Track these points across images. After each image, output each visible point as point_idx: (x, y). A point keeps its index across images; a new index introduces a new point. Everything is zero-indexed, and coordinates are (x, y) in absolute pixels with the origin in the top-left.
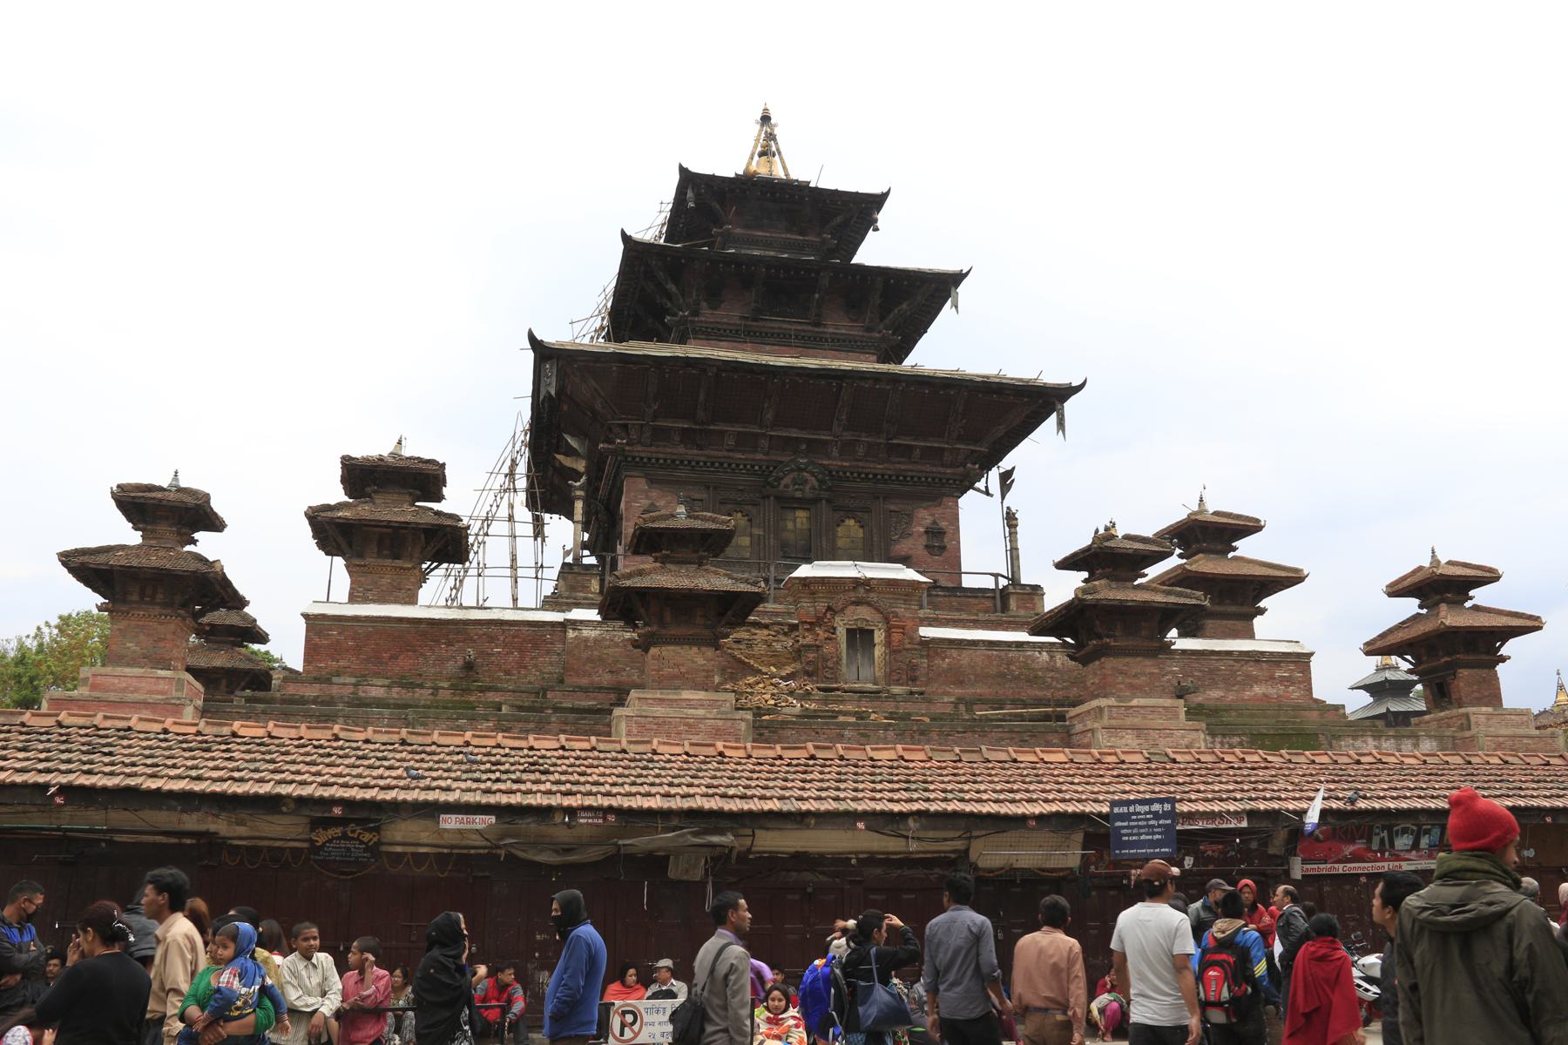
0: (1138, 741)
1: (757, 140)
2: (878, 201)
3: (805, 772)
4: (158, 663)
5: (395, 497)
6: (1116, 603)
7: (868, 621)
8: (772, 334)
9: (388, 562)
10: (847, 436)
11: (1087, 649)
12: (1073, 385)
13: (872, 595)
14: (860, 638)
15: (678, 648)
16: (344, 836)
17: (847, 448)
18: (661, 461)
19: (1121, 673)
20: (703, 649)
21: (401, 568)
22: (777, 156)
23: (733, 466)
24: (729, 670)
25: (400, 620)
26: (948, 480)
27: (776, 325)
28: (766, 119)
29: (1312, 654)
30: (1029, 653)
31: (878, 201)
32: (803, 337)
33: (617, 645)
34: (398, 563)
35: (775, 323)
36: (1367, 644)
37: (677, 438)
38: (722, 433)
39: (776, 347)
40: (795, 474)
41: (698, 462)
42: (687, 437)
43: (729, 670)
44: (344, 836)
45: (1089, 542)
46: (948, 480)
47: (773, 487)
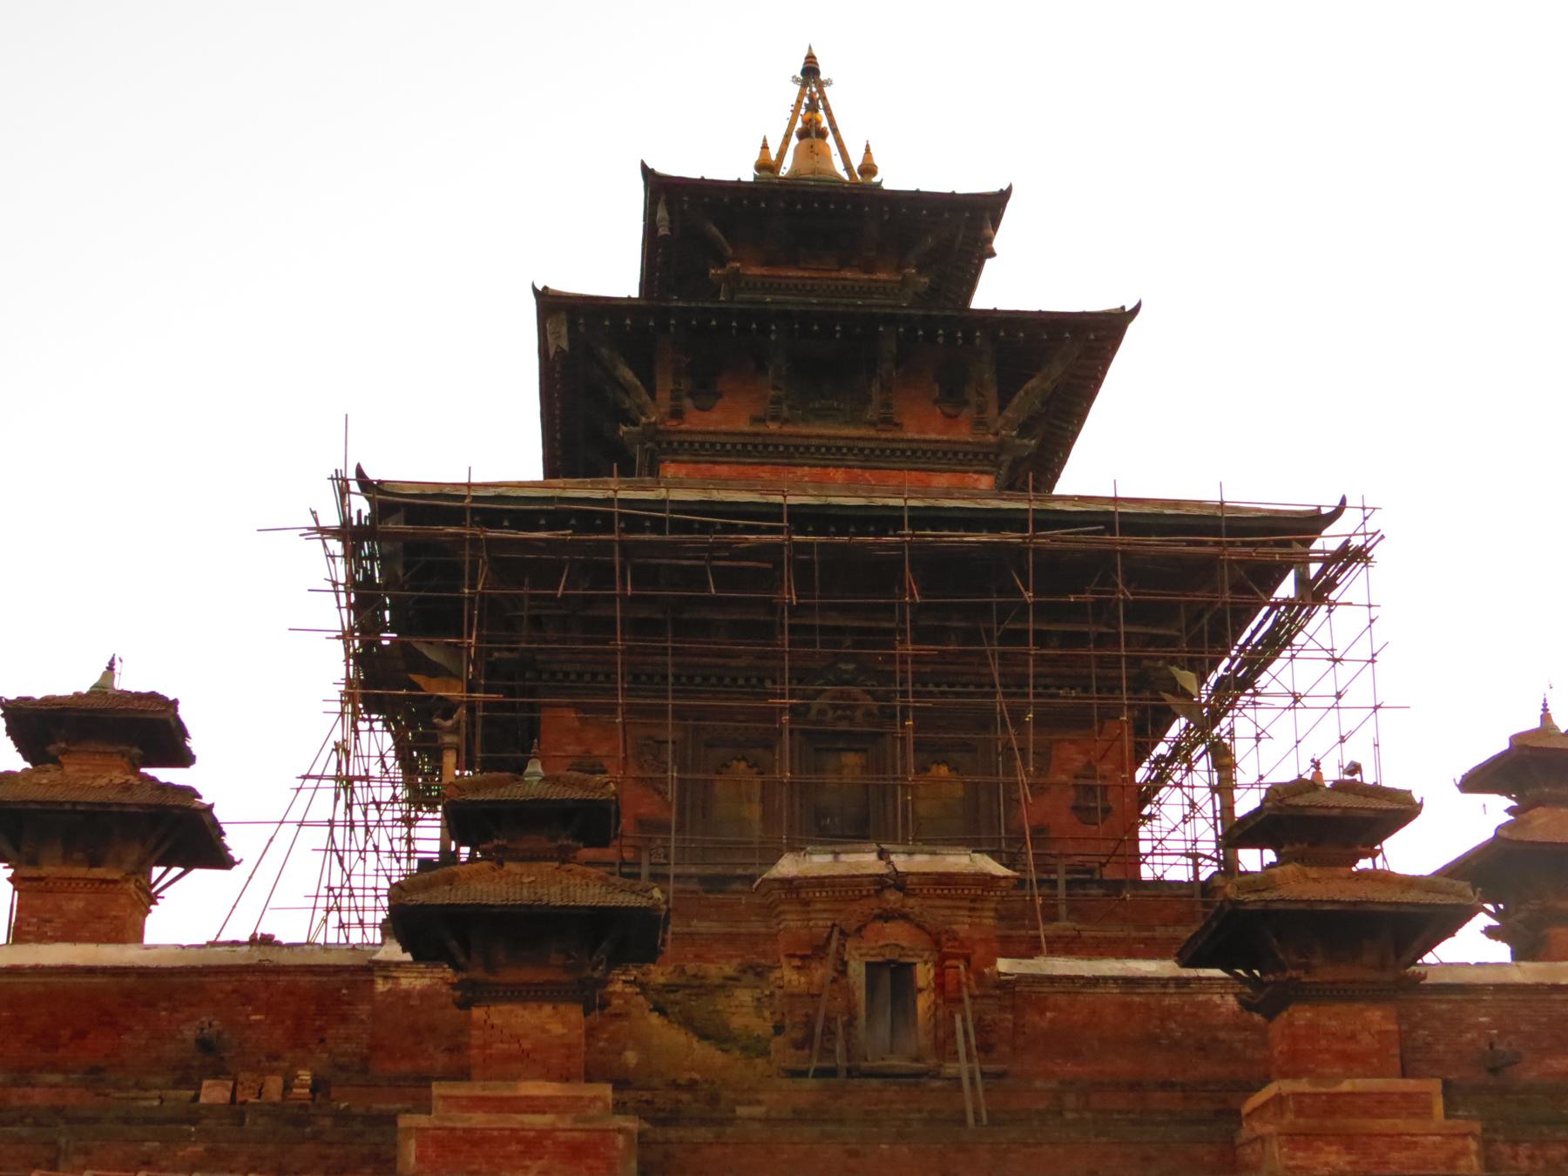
0: (1349, 1158)
1: (795, 112)
2: (989, 208)
6: (1301, 906)
7: (903, 948)
8: (807, 448)
12: (1325, 511)
13: (911, 902)
20: (562, 1007)
21: (103, 881)
22: (830, 140)
28: (810, 70)
30: (1201, 998)
32: (862, 450)
34: (98, 872)
39: (815, 470)
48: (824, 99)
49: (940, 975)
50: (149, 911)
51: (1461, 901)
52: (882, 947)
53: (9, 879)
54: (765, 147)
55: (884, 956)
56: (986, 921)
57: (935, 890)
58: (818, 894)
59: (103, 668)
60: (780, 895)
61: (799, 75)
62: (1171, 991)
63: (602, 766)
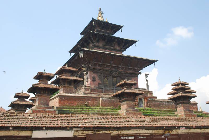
3: (65, 121)
4: (47, 105)
5: (68, 75)
9: (69, 86)
10: (123, 66)
11: (121, 100)
16: (168, 132)
17: (122, 68)
19: (185, 106)
25: (74, 96)
27: (108, 47)
29: (197, 103)
31: (122, 27)
33: (108, 101)
34: (70, 86)
35: (108, 47)
37: (97, 65)
38: (104, 65)
40: (115, 72)
42: (99, 65)
44: (168, 132)
47: (112, 74)
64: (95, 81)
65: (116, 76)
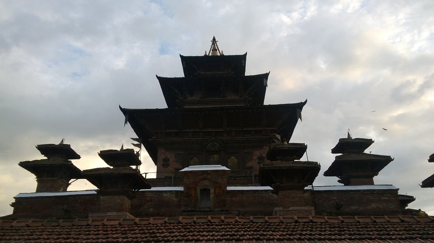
7: (207, 186)
12: (303, 102)
13: (209, 176)
14: (205, 192)
15: (111, 197)
18: (168, 143)
20: (120, 196)
22: (218, 50)
23: (192, 142)
24: (156, 206)
26: (265, 140)
28: (214, 39)
36: (423, 182)
40: (212, 143)
41: (180, 142)
43: (156, 206)
45: (335, 160)
46: (265, 140)
48: (216, 44)
49: (215, 191)
50: (68, 187)
51: (315, 166)
52: (204, 185)
53: (36, 181)
54: (206, 52)
55: (203, 187)
56: (225, 180)
57: (214, 173)
58: (190, 175)
59: (61, 141)
60: (183, 175)
61: (212, 40)
62: (264, 193)
63: (168, 159)
64: (169, 165)
65: (214, 151)
